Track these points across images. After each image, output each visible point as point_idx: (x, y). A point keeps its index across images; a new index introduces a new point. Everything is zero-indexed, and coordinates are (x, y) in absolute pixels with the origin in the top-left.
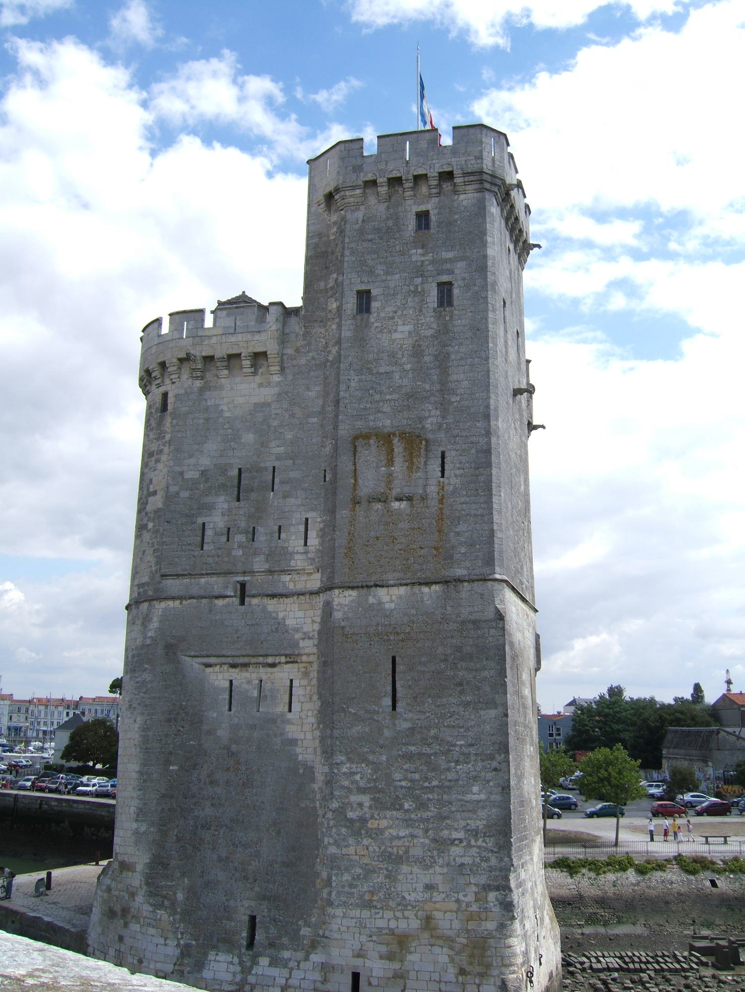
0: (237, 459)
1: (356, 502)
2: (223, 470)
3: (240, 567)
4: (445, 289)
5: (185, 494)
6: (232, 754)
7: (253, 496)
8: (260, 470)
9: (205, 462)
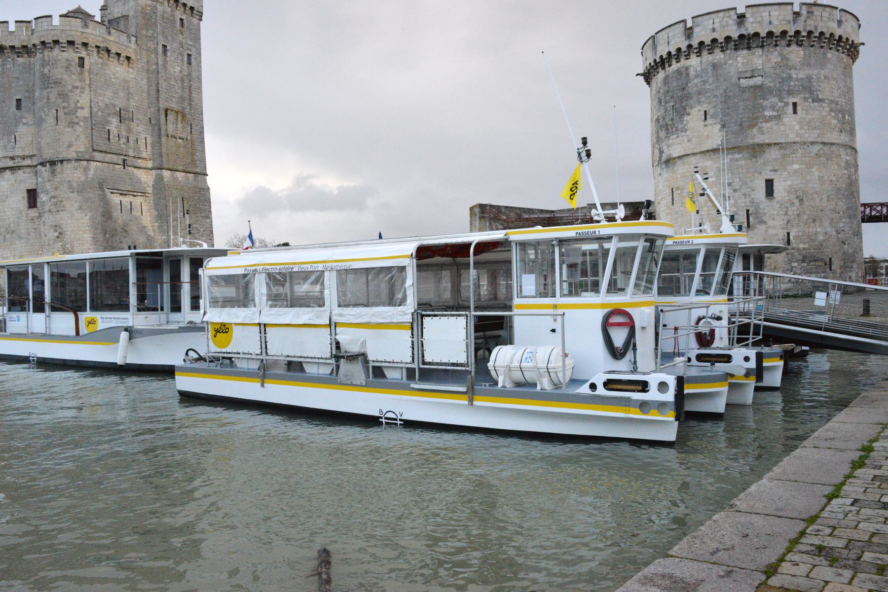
0: (119, 103)
1: (167, 136)
2: (114, 106)
3: (124, 153)
4: (189, 55)
5: (100, 113)
6: (126, 231)
7: (127, 122)
8: (128, 111)
9: (107, 101)
